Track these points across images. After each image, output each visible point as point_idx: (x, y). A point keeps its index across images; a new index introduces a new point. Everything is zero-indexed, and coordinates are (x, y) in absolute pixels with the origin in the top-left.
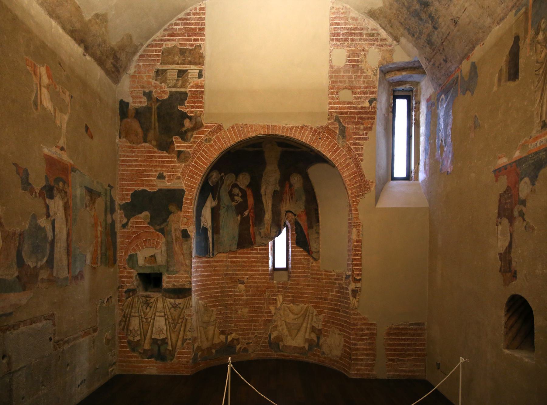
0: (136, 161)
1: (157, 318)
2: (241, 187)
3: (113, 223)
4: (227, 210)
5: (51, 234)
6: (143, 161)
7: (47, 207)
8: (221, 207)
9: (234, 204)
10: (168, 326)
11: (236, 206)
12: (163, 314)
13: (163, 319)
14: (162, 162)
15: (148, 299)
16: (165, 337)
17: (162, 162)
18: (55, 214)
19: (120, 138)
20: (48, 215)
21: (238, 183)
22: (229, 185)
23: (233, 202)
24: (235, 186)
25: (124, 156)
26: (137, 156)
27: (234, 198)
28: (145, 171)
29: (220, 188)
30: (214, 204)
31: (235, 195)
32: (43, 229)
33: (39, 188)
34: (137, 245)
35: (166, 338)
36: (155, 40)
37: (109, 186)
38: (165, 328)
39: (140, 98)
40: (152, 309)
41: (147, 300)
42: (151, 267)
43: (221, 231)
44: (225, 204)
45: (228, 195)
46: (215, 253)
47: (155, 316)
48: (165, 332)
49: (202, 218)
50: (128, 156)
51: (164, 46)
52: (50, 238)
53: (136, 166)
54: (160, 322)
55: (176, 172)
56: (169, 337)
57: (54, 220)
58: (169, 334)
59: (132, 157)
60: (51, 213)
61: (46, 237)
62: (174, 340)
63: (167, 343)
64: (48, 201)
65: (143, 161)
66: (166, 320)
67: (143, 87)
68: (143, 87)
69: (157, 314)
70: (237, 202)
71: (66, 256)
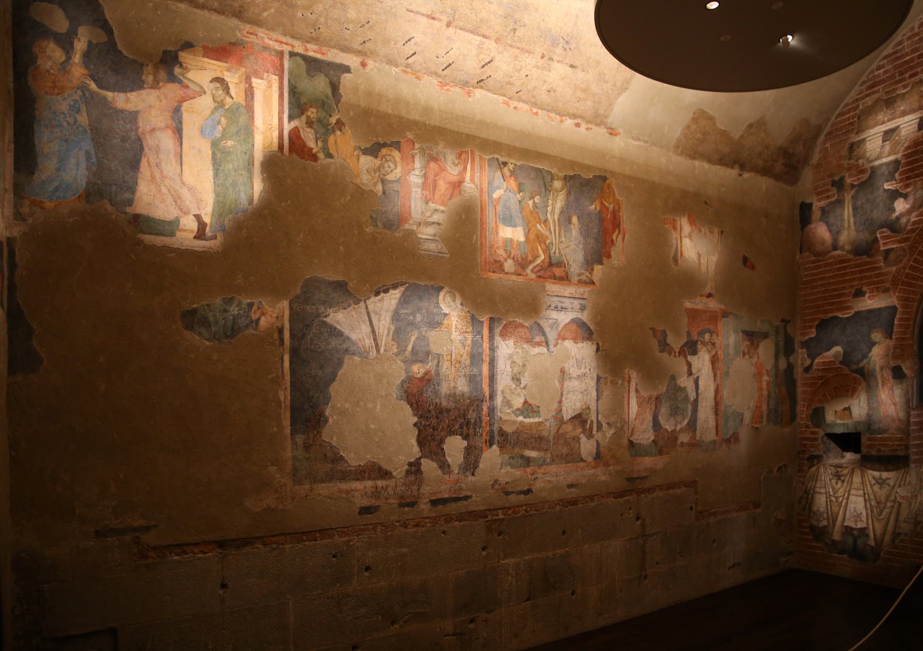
0: (823, 279)
1: (852, 498)
3: (790, 368)
5: (694, 394)
6: (833, 277)
7: (689, 365)
10: (869, 511)
12: (861, 492)
13: (861, 499)
14: (861, 272)
15: (839, 469)
16: (864, 525)
17: (861, 272)
18: (699, 370)
19: (801, 252)
20: (690, 373)
25: (806, 276)
26: (825, 272)
28: (835, 290)
32: (683, 390)
33: (679, 346)
34: (824, 395)
35: (865, 529)
36: (847, 105)
37: (783, 320)
38: (864, 513)
39: (828, 191)
40: (845, 484)
41: (837, 472)
42: (844, 424)
47: (849, 494)
48: (864, 519)
50: (812, 275)
51: (861, 107)
52: (692, 396)
53: (822, 285)
54: (857, 504)
55: (883, 281)
56: (871, 527)
57: (698, 377)
58: (870, 521)
59: (817, 274)
60: (694, 371)
61: (686, 398)
62: (879, 532)
63: (867, 536)
64: (689, 358)
65: (833, 277)
66: (865, 500)
67: (831, 176)
68: (831, 176)
69: (853, 492)
71: (713, 417)
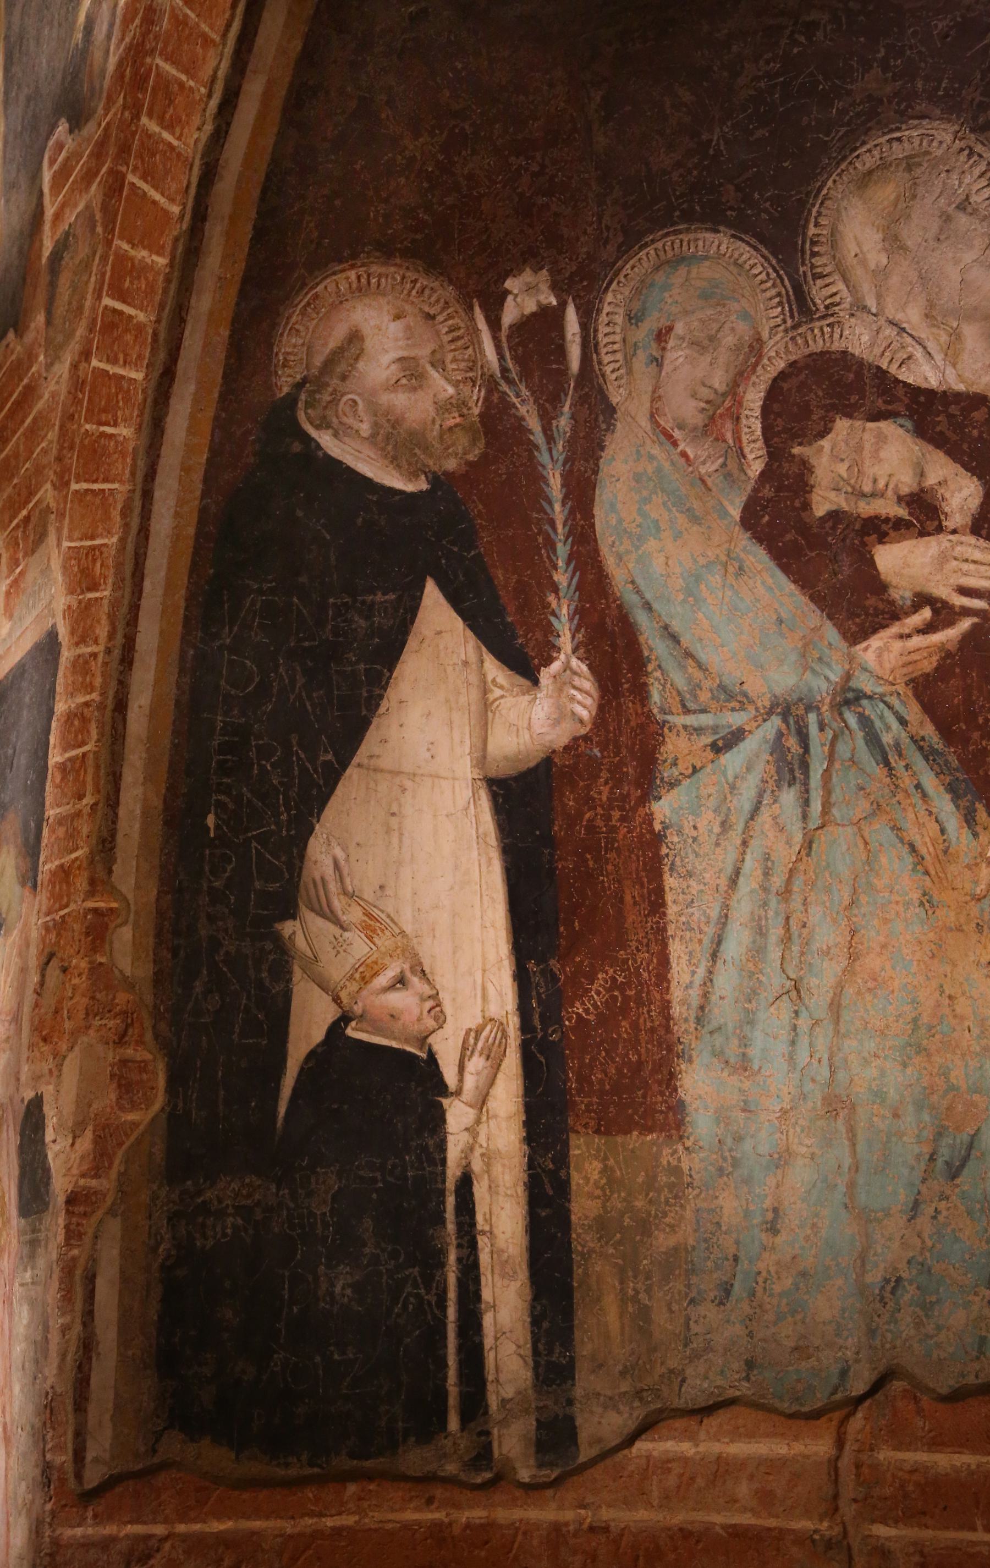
2: (926, 373)
4: (791, 767)
8: (675, 747)
9: (888, 655)
11: (925, 688)
21: (859, 339)
22: (719, 414)
23: (857, 634)
24: (823, 390)
27: (877, 585)
29: (581, 493)
30: (544, 714)
31: (881, 529)
43: (699, 1083)
44: (733, 696)
45: (757, 557)
46: (599, 1424)
49: (304, 932)
70: (944, 613)
